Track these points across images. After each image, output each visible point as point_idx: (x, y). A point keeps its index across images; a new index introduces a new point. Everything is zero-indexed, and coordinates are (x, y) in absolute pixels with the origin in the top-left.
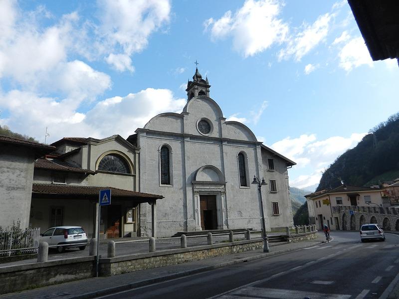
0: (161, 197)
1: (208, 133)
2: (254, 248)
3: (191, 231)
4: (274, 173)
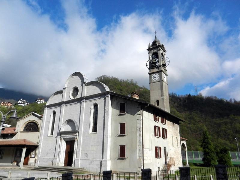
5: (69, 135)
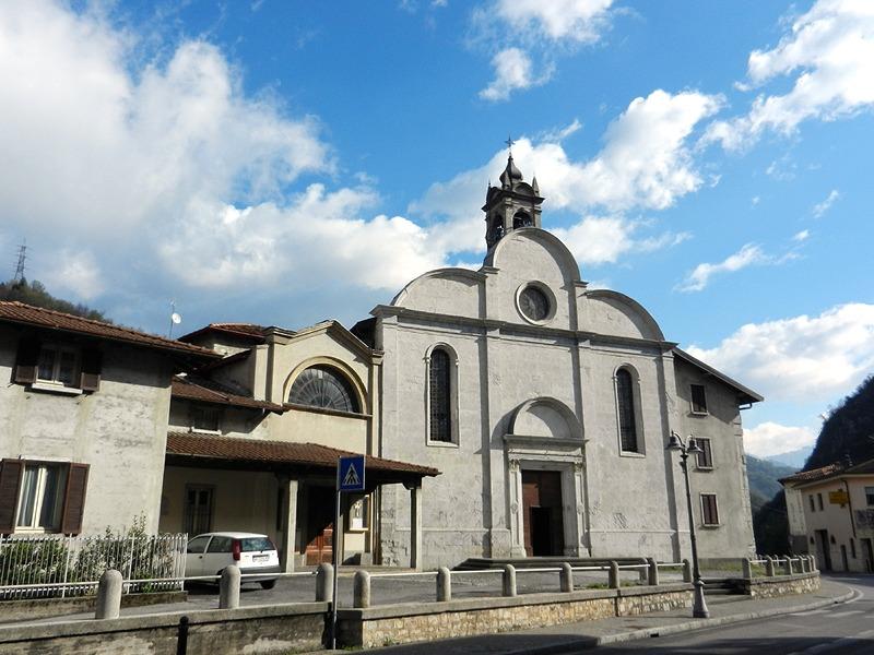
0: (434, 473)
1: (543, 317)
2: (666, 607)
3: (501, 558)
4: (704, 421)
5: (550, 452)
